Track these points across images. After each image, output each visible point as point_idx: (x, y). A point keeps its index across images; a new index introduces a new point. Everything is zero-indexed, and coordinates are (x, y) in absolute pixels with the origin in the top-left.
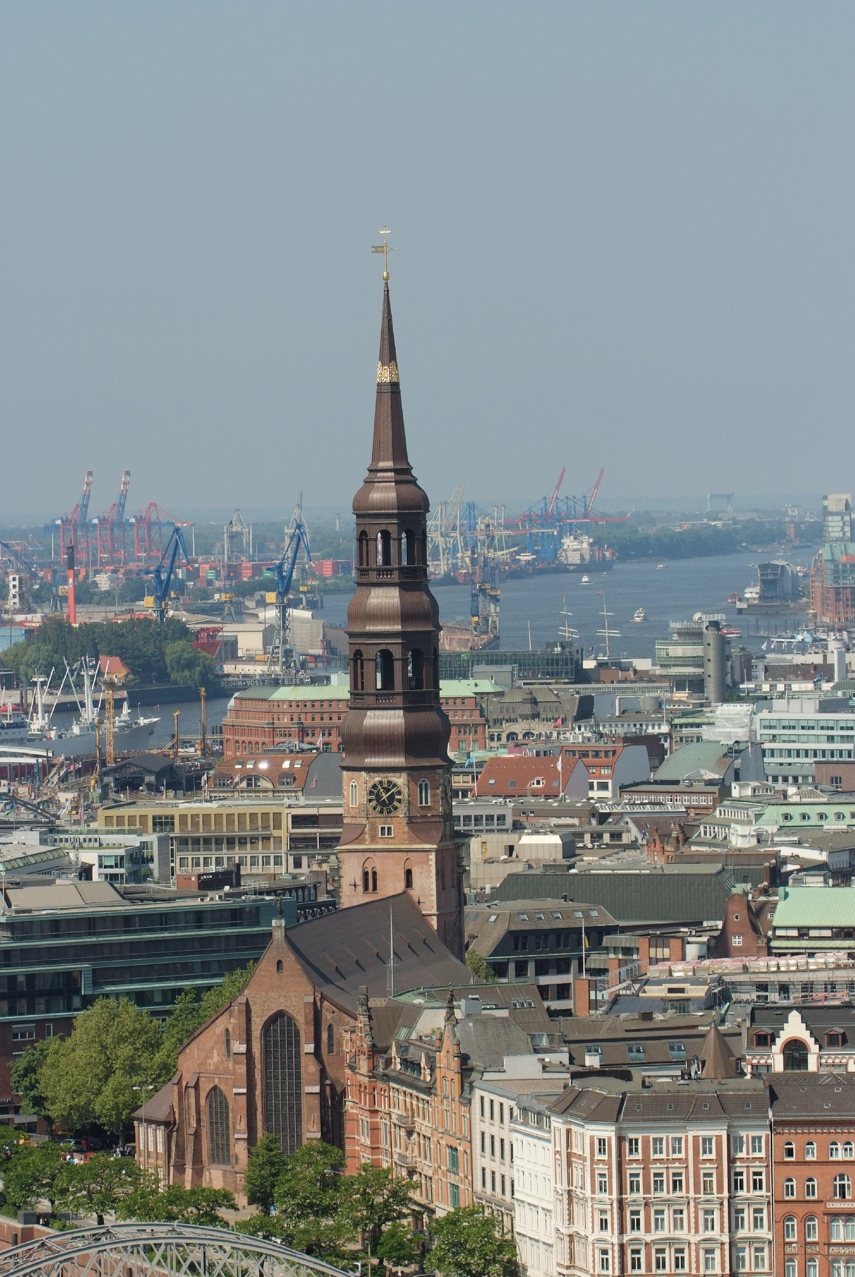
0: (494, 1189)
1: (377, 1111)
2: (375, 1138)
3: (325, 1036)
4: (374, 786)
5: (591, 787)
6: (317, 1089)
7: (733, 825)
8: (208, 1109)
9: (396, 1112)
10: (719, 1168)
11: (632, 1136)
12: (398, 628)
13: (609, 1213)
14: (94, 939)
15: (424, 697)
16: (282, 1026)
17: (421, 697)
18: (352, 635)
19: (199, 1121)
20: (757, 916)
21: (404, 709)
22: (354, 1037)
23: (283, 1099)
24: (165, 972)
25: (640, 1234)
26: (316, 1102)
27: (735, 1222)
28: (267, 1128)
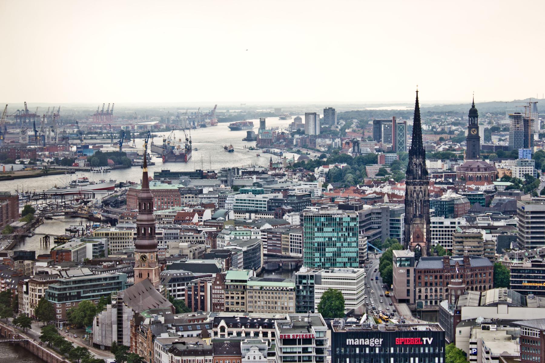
2: (136, 344)
9: (140, 340)
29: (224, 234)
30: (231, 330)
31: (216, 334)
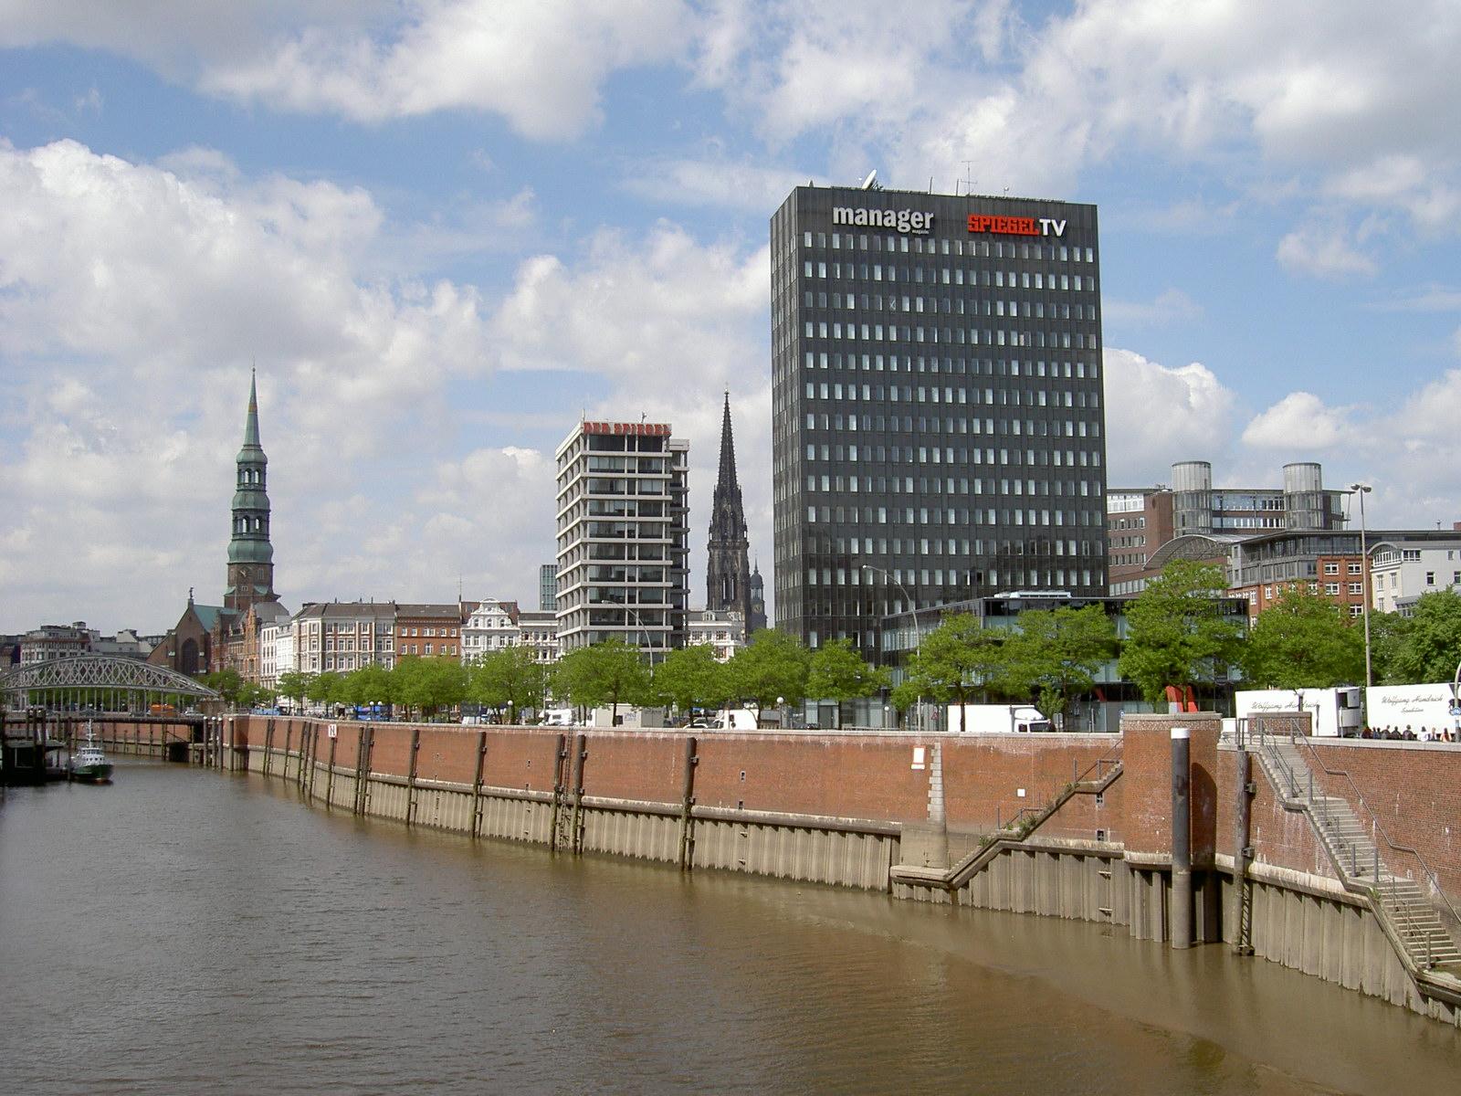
10: (370, 639)
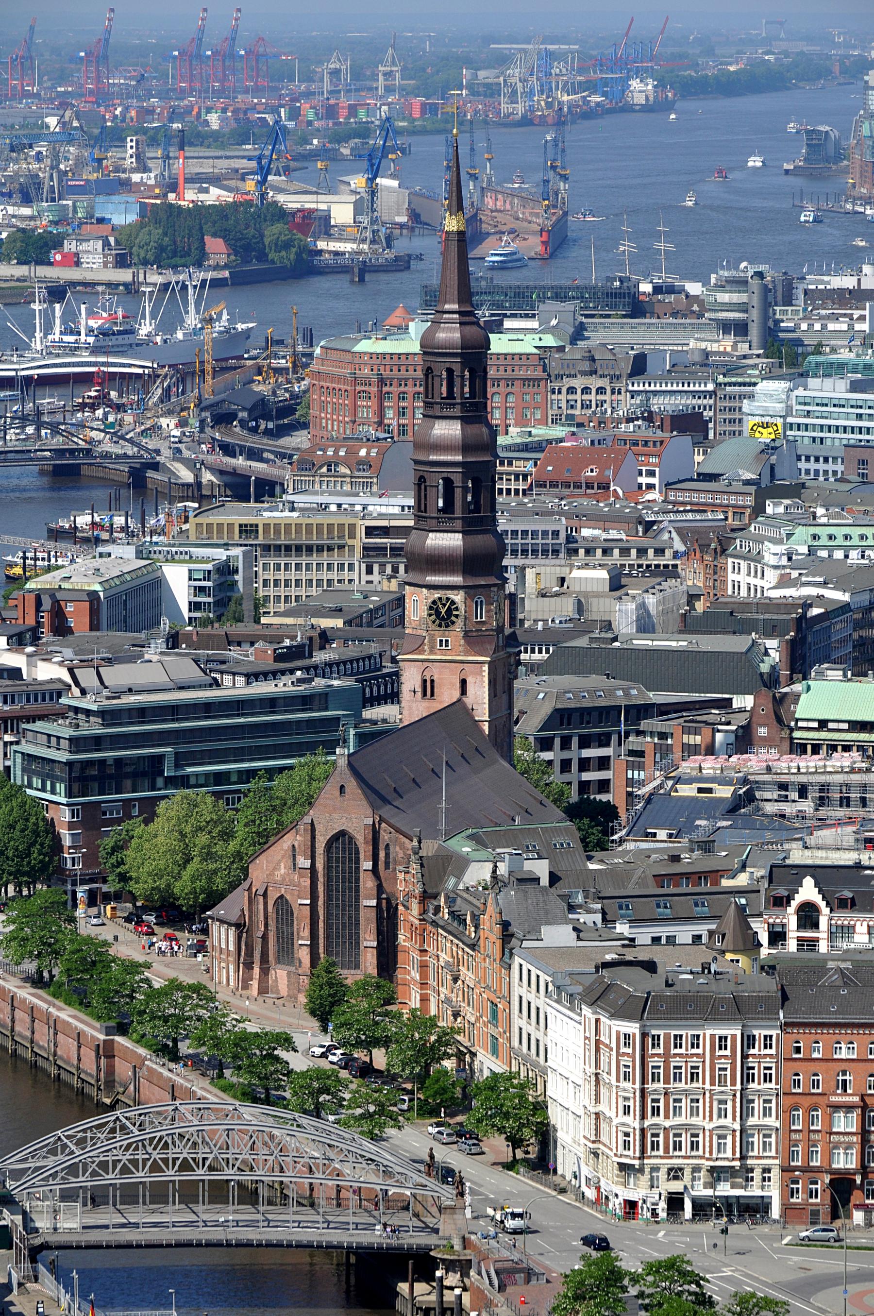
0: (529, 1048)
1: (426, 951)
2: (424, 975)
3: (382, 854)
4: (434, 602)
5: (640, 473)
6: (374, 903)
7: (766, 543)
8: (275, 915)
9: (444, 957)
11: (654, 1032)
12: (459, 458)
13: (632, 1100)
14: (177, 725)
15: (481, 521)
16: (344, 843)
17: (479, 517)
18: (416, 462)
19: (266, 925)
20: (780, 709)
21: (464, 533)
22: (408, 877)
23: (344, 910)
24: (239, 755)
25: (660, 1120)
26: (373, 914)
27: (746, 1112)
28: (328, 953)
29: (760, 540)
30: (844, 918)
31: (777, 937)
